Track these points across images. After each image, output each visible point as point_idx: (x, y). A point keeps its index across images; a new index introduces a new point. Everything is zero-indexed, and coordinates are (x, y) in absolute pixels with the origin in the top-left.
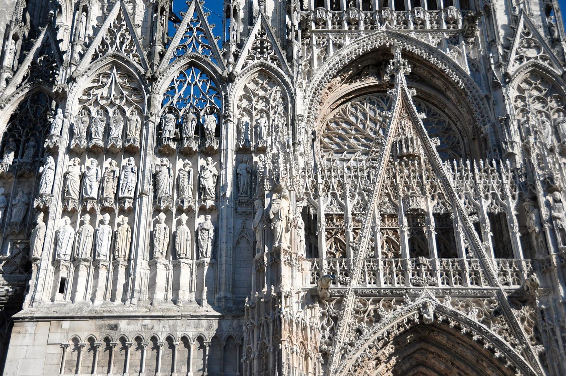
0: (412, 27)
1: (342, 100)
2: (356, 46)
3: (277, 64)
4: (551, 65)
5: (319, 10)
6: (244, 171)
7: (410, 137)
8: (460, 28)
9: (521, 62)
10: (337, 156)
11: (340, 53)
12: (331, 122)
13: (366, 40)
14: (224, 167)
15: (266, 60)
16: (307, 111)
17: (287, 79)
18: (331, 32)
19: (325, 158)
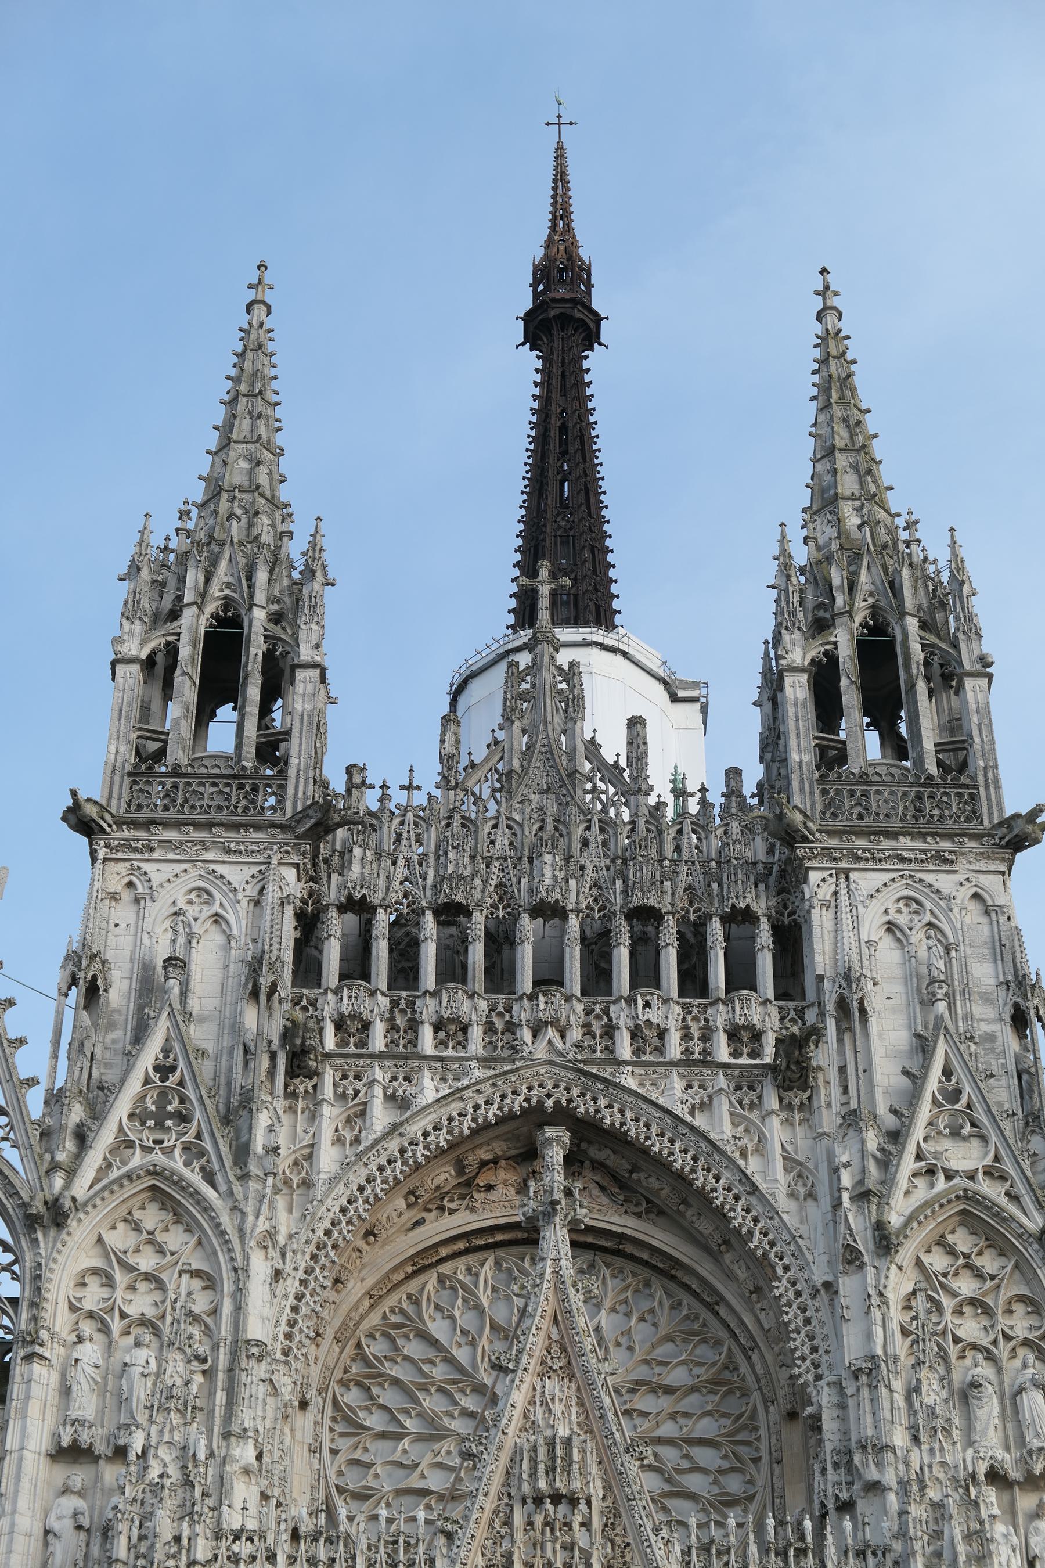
0: (625, 1049)
1: (409, 1269)
2: (454, 1108)
3: (202, 1169)
4: (1011, 1196)
5: (349, 987)
6: (63, 1526)
7: (563, 1431)
8: (768, 1060)
9: (932, 1185)
10: (378, 1451)
11: (402, 1130)
12: (371, 1336)
13: (487, 1087)
14: (8, 1508)
15: (169, 1152)
16: (284, 1318)
17: (226, 1220)
18: (380, 1056)
19: (342, 1458)
